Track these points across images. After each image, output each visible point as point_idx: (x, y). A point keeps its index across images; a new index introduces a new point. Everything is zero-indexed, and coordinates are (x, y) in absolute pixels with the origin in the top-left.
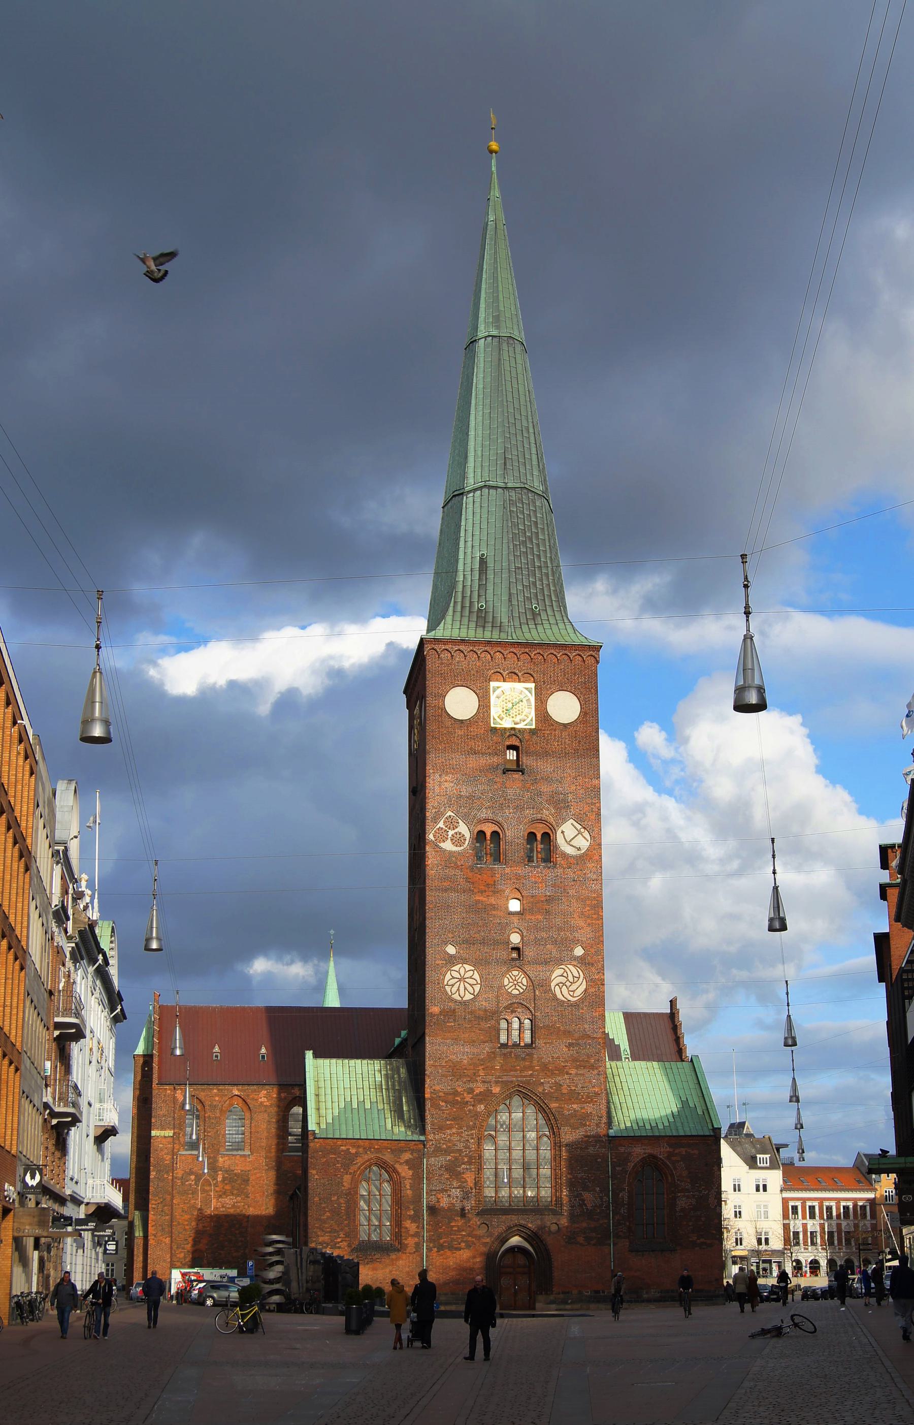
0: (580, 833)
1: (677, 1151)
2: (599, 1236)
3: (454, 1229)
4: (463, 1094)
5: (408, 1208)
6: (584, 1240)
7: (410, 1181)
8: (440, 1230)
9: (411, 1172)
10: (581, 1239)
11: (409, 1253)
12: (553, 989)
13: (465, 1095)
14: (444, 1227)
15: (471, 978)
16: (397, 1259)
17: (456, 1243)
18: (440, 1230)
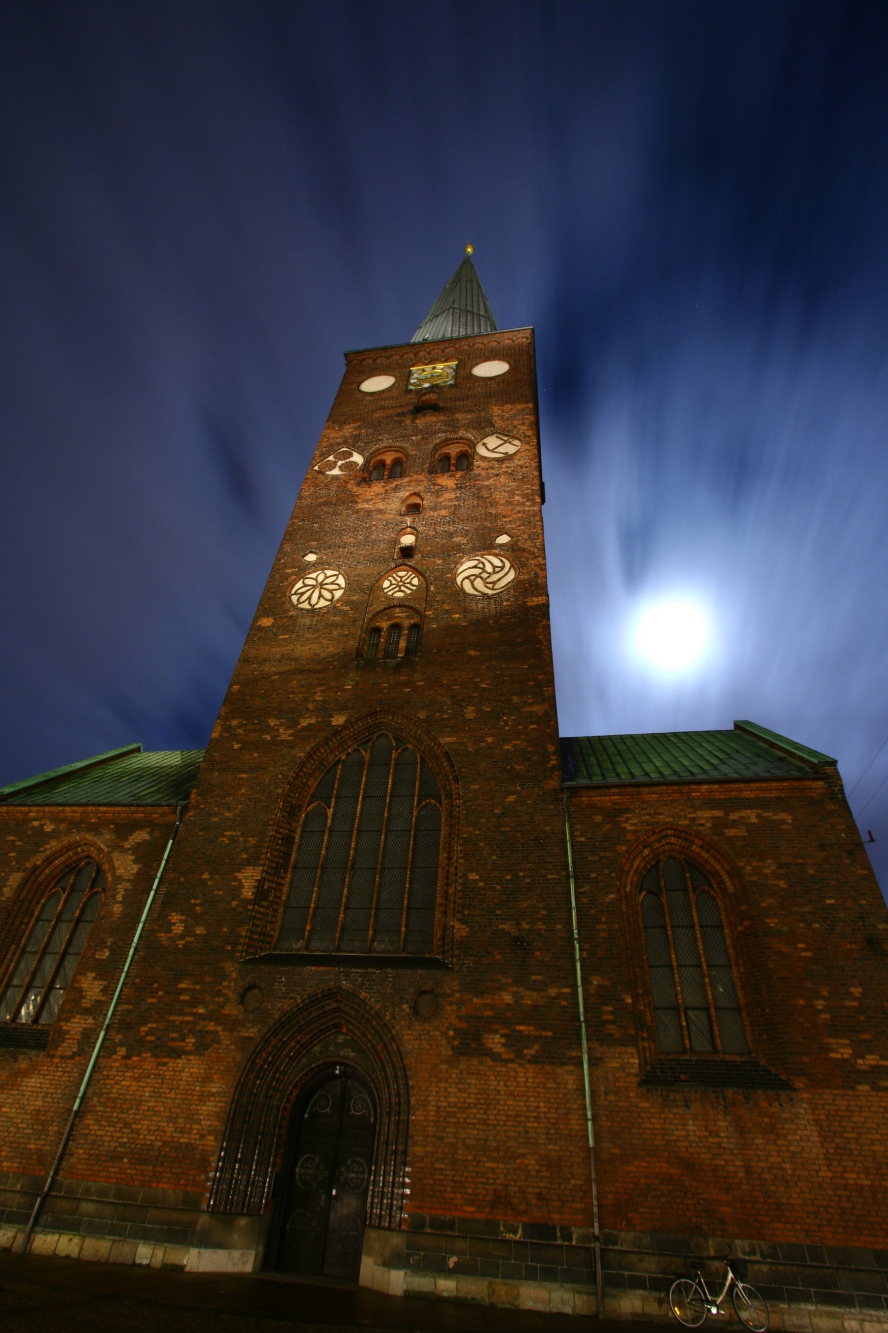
0: (505, 442)
1: (734, 816)
2: (549, 1034)
3: (182, 998)
4: (278, 730)
5: (101, 945)
6: (505, 1045)
7: (128, 885)
8: (150, 1000)
9: (135, 868)
10: (495, 1042)
11: (61, 1057)
12: (459, 583)
13: (281, 730)
14: (161, 993)
15: (332, 583)
16: (33, 1069)
17: (175, 1035)
18: (150, 1000)
